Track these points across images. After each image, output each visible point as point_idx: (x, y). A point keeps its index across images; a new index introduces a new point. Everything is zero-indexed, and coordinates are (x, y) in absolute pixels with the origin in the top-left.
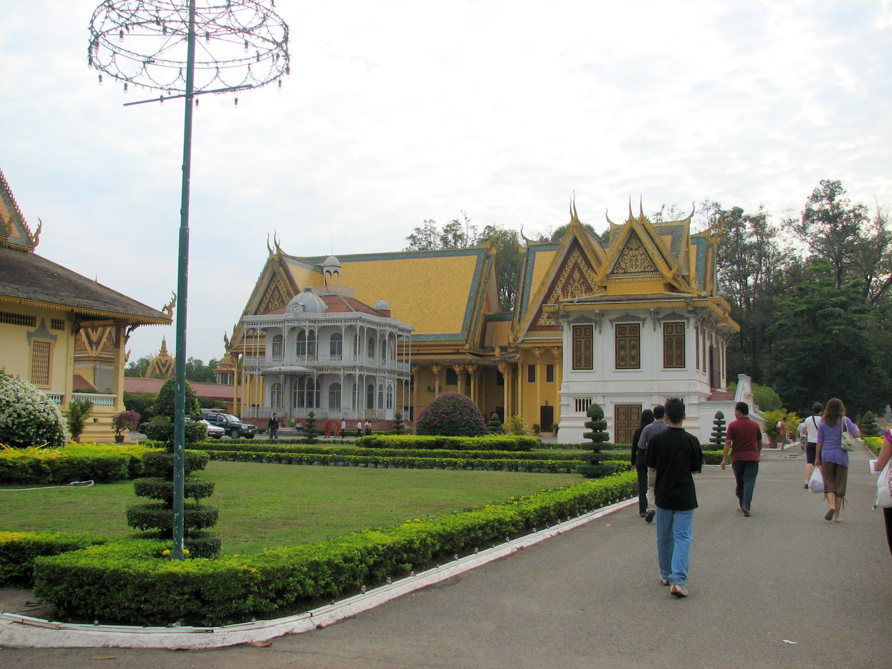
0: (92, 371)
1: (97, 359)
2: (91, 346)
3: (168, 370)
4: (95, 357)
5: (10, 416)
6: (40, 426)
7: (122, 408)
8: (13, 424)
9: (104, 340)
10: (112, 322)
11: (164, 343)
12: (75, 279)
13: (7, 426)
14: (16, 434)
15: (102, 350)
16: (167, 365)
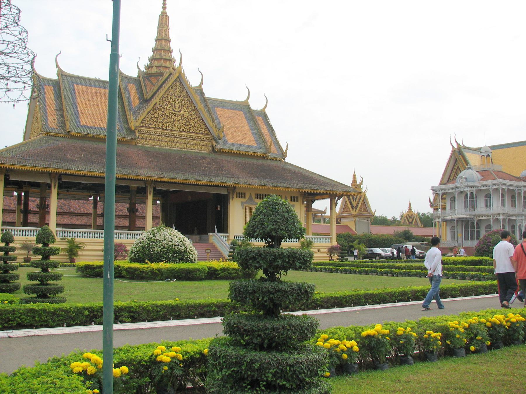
0: (354, 223)
1: (356, 216)
2: (353, 209)
3: (413, 220)
4: (355, 215)
5: (160, 247)
6: (175, 252)
7: (335, 243)
8: (161, 251)
9: (360, 205)
10: (328, 196)
11: (410, 204)
12: (304, 173)
13: (158, 252)
14: (162, 256)
15: (359, 211)
16: (412, 218)
